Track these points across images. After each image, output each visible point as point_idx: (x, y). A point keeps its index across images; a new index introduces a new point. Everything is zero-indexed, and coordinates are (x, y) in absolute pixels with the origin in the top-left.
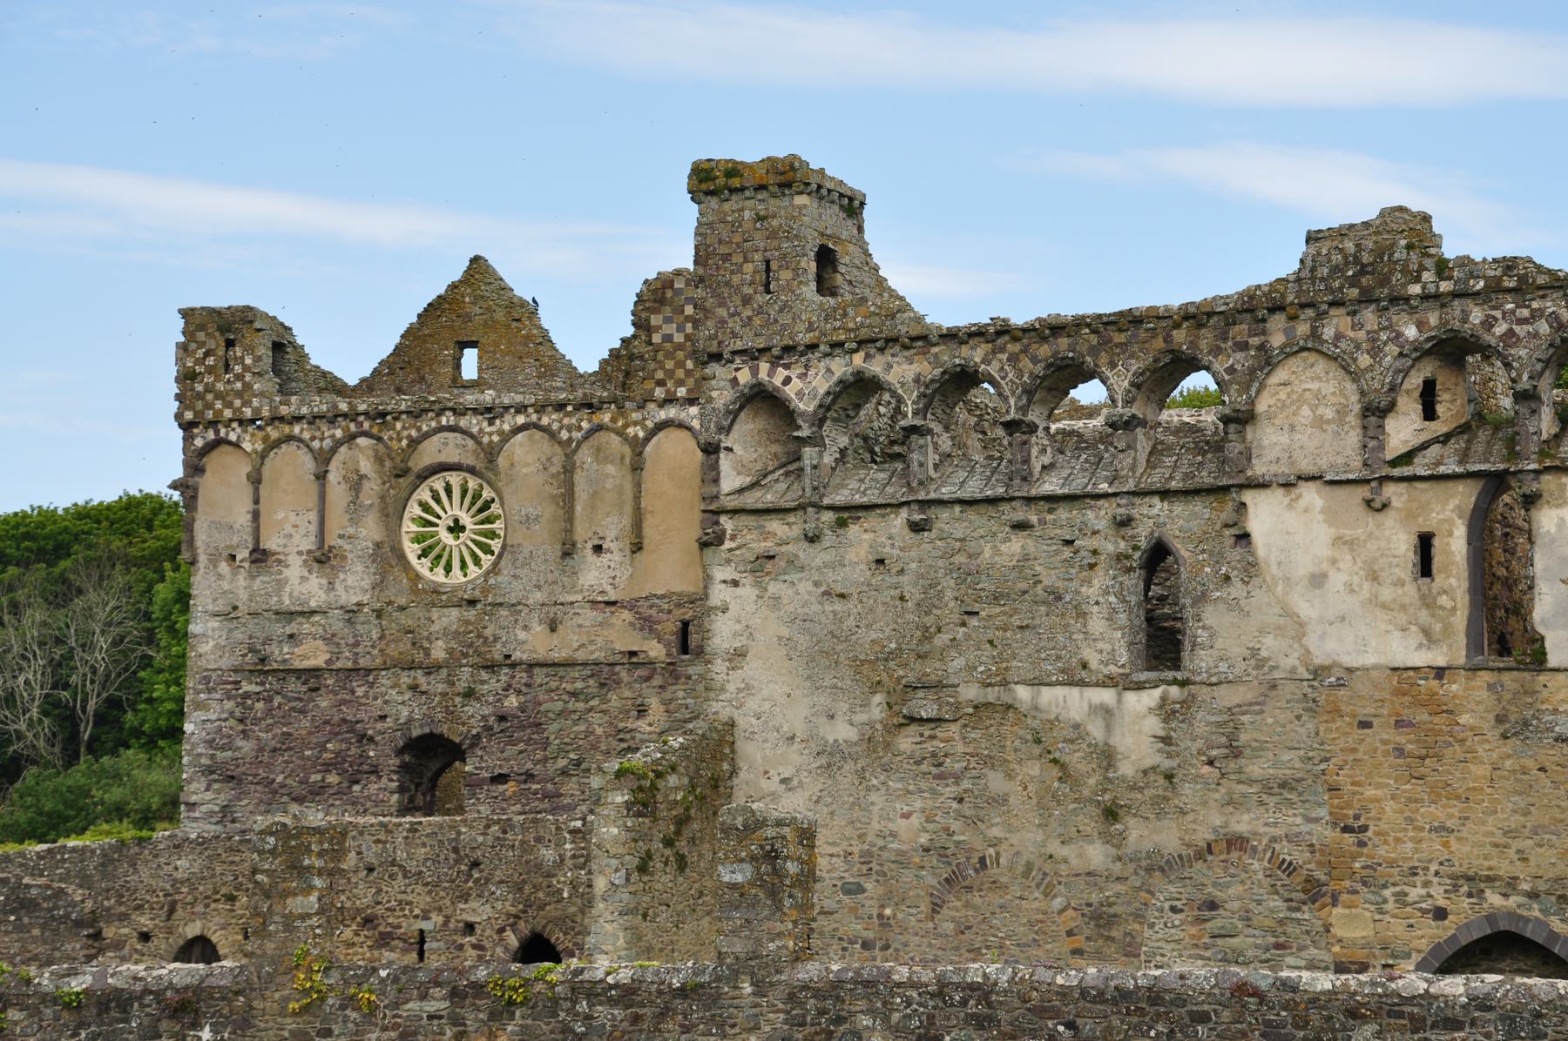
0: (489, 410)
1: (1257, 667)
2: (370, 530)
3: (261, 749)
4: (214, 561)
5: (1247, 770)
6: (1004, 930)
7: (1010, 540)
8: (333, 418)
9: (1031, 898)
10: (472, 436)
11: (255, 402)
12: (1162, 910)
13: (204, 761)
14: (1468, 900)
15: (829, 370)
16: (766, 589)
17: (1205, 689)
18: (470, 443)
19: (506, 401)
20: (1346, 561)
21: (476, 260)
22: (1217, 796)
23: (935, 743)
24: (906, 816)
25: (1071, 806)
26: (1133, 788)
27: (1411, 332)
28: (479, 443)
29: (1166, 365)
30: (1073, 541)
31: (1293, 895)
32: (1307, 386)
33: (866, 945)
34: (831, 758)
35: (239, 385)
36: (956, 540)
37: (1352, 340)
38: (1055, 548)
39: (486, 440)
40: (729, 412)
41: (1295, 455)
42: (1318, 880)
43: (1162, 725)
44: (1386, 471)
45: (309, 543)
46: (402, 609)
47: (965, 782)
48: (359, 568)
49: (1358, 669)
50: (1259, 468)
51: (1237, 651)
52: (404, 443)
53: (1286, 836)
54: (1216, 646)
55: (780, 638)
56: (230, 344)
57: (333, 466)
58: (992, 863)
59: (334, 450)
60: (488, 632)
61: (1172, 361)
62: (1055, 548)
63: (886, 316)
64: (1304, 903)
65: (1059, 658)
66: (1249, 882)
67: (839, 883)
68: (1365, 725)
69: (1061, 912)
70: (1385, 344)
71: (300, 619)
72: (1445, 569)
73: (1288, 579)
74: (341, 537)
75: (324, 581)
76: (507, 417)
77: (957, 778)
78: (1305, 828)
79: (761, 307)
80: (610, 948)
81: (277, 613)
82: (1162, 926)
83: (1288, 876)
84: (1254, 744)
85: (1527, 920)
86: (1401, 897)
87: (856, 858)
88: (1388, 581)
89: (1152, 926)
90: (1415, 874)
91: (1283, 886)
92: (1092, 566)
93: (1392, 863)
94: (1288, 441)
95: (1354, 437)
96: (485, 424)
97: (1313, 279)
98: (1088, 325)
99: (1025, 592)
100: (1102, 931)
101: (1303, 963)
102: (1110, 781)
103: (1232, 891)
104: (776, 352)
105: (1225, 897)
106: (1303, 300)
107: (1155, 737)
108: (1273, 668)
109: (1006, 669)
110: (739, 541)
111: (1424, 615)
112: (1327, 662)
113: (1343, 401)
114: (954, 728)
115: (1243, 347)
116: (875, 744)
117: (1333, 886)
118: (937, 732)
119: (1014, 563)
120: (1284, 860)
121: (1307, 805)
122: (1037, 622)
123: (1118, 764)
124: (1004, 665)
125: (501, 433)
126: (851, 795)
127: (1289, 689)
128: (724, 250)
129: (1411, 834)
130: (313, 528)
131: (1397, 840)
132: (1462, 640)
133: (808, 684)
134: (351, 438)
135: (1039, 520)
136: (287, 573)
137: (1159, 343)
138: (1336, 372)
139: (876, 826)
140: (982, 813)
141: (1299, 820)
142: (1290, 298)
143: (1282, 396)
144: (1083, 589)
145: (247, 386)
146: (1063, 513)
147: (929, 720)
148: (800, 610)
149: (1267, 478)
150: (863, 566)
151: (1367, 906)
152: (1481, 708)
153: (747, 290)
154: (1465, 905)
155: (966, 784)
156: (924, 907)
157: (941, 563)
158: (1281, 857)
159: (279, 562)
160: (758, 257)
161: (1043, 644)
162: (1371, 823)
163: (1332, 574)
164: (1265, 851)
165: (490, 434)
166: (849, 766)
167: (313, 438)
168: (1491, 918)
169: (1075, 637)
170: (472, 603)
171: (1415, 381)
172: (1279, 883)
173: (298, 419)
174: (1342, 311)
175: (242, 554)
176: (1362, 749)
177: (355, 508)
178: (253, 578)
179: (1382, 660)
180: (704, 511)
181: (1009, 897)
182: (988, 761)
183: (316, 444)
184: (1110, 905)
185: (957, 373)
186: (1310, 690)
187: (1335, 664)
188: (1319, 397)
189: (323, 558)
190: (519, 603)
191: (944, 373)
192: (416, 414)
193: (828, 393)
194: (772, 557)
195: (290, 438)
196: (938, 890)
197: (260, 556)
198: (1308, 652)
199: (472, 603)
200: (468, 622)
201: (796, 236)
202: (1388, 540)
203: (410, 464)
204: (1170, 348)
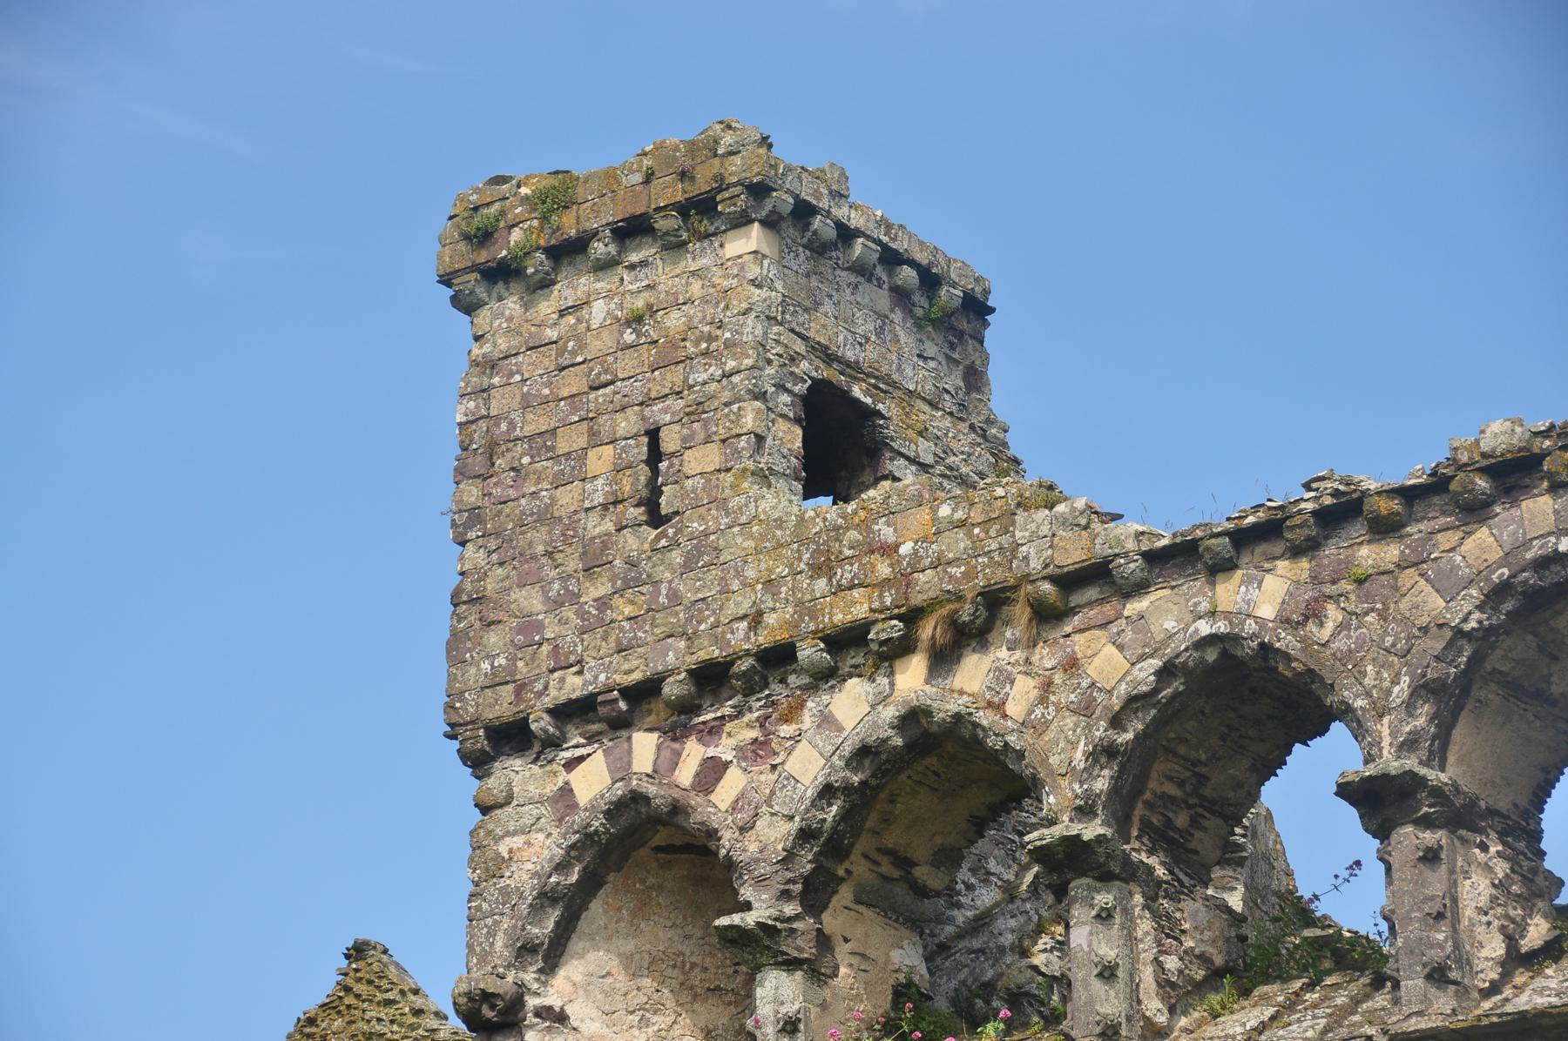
15: (827, 720)
21: (358, 951)
40: (546, 898)
104: (671, 689)
128: (537, 422)
153: (598, 526)
160: (627, 424)
185: (1209, 671)
193: (827, 792)
201: (728, 344)
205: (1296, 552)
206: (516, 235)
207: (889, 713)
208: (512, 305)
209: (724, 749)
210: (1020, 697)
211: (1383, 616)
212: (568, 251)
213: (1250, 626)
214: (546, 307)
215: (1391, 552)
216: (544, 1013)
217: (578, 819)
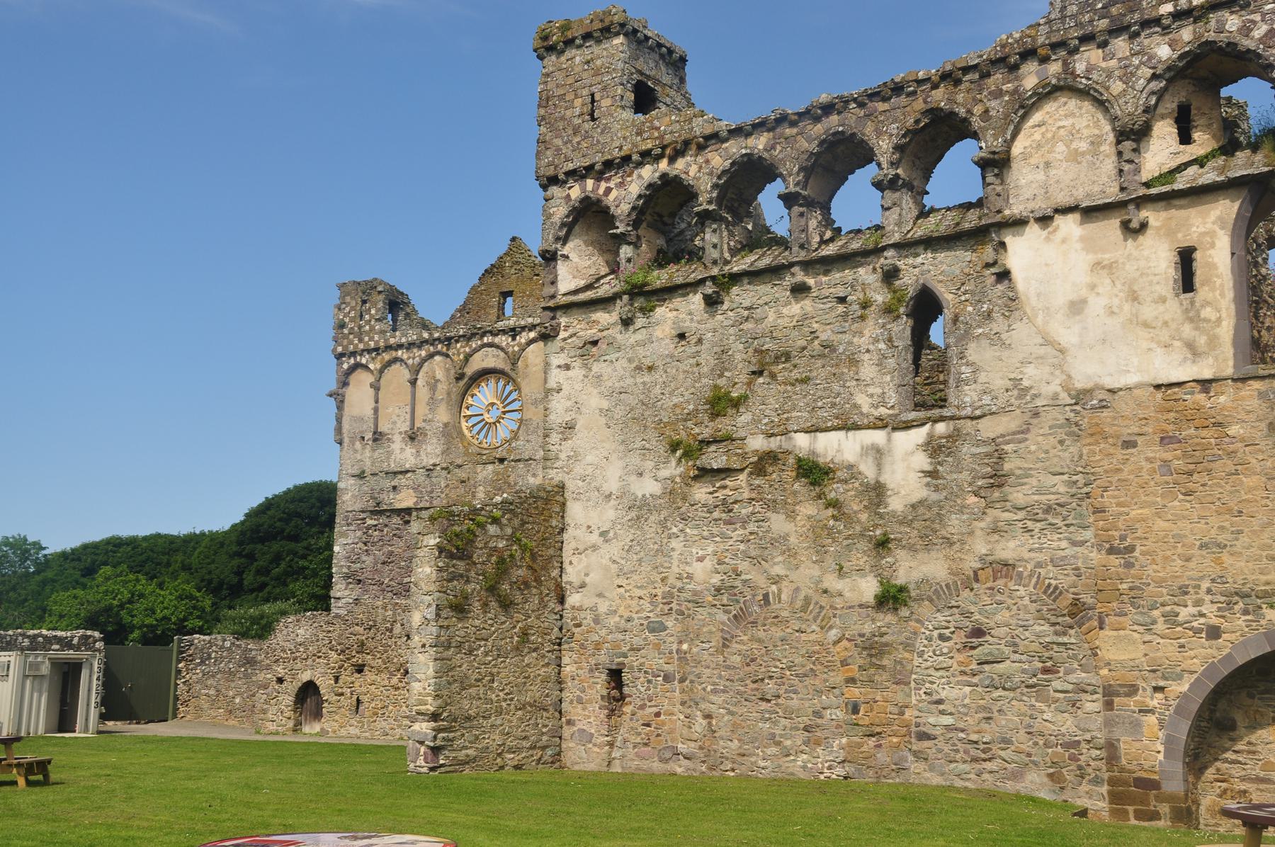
0: (513, 330)
1: (1020, 397)
2: (443, 415)
3: (376, 563)
4: (352, 443)
5: (1010, 497)
6: (784, 661)
7: (790, 304)
8: (422, 343)
9: (809, 631)
10: (502, 349)
11: (376, 338)
12: (930, 639)
13: (345, 570)
14: (1244, 618)
15: (640, 176)
16: (590, 369)
17: (969, 423)
18: (502, 354)
19: (523, 323)
20: (1105, 284)
21: (514, 239)
22: (982, 525)
23: (727, 492)
24: (700, 559)
25: (846, 542)
26: (903, 521)
27: (1164, 52)
28: (506, 353)
29: (926, 125)
30: (846, 297)
31: (1060, 620)
32: (1061, 124)
33: (667, 678)
34: (639, 509)
35: (367, 327)
36: (747, 309)
37: (1103, 70)
38: (830, 305)
39: (510, 349)
40: (563, 225)
41: (1050, 190)
42: (1084, 604)
43: (929, 460)
44: (1142, 191)
45: (405, 427)
46: (459, 466)
47: (751, 525)
48: (435, 441)
49: (1121, 389)
50: (1015, 209)
51: (999, 383)
52: (462, 357)
53: (1052, 561)
54: (980, 380)
55: (601, 410)
56: (364, 302)
57: (420, 376)
58: (774, 599)
59: (421, 365)
60: (511, 479)
61: (932, 122)
62: (830, 305)
63: (685, 121)
64: (1071, 627)
65: (834, 405)
66: (1015, 608)
67: (645, 623)
68: (1129, 444)
69: (836, 643)
70: (1137, 68)
71: (400, 476)
72: (1207, 282)
73: (1048, 308)
74: (424, 421)
75: (414, 451)
76: (524, 334)
77: (744, 523)
78: (1070, 551)
79: (587, 132)
80: (423, 676)
81: (387, 473)
82: (931, 654)
83: (1054, 601)
84: (1018, 472)
86: (1171, 618)
87: (659, 598)
88: (1149, 299)
89: (921, 654)
90: (1186, 593)
91: (1049, 610)
92: (863, 318)
93: (1160, 583)
94: (1044, 178)
95: (1109, 165)
96: (510, 339)
97: (1063, 18)
98: (855, 100)
99: (804, 348)
100: (874, 660)
101: (1070, 687)
102: (881, 516)
103: (998, 618)
104: (597, 167)
105: (992, 624)
106: (1054, 40)
107: (923, 472)
108: (1035, 396)
109: (787, 419)
110: (571, 331)
111: (1187, 330)
112: (1089, 385)
113: (1097, 132)
114: (743, 477)
115: (998, 94)
116: (674, 495)
117: (1100, 608)
118: (727, 482)
119: (794, 323)
120: (1049, 585)
121: (1072, 529)
122: (814, 374)
123: (889, 500)
124: (785, 416)
125: (519, 344)
126: (656, 543)
127: (1052, 416)
128: (561, 92)
129: (1180, 550)
130: (408, 416)
131: (1166, 558)
132: (1228, 350)
133: (622, 448)
134: (431, 356)
135: (816, 282)
136: (393, 446)
137: (919, 105)
138: (1087, 105)
139: (675, 569)
140: (767, 552)
141: (1064, 544)
142: (1041, 40)
143: (1037, 136)
144: (855, 340)
145: (372, 329)
146: (836, 276)
147: (719, 471)
148: (617, 385)
149: (1025, 214)
150: (667, 341)
151: (1136, 627)
152: (1252, 417)
153: (577, 121)
155: (752, 527)
156: (716, 641)
157: (732, 331)
158: (1047, 581)
159: (389, 440)
160: (585, 92)
161: (820, 393)
162: (1138, 543)
163: (1092, 300)
164: (1031, 576)
165: (513, 346)
166: (654, 518)
167: (409, 358)
169: (848, 384)
170: (502, 460)
171: (1170, 105)
173: (400, 346)
174: (1092, 46)
175: (369, 436)
176: (1127, 468)
177: (432, 403)
178: (374, 450)
179: (1147, 378)
180: (545, 309)
181: (789, 630)
182: (772, 505)
183: (410, 362)
184: (882, 635)
186: (1072, 415)
187: (1098, 387)
188: (1073, 133)
189: (413, 437)
190: (531, 459)
191: (733, 164)
192: (468, 338)
193: (640, 196)
194: (595, 343)
195: (396, 360)
196: (728, 626)
197: (378, 437)
198: (1069, 377)
199: (502, 460)
200: (497, 474)
202: (1148, 259)
203: (465, 370)
204: (929, 106)
205: (769, 130)
206: (555, 38)
207: (657, 175)
208: (554, 58)
209: (612, 184)
210: (693, 170)
211: (792, 148)
212: (569, 43)
213: (756, 151)
214: (563, 59)
215: (795, 131)
216: (563, 256)
217: (572, 203)
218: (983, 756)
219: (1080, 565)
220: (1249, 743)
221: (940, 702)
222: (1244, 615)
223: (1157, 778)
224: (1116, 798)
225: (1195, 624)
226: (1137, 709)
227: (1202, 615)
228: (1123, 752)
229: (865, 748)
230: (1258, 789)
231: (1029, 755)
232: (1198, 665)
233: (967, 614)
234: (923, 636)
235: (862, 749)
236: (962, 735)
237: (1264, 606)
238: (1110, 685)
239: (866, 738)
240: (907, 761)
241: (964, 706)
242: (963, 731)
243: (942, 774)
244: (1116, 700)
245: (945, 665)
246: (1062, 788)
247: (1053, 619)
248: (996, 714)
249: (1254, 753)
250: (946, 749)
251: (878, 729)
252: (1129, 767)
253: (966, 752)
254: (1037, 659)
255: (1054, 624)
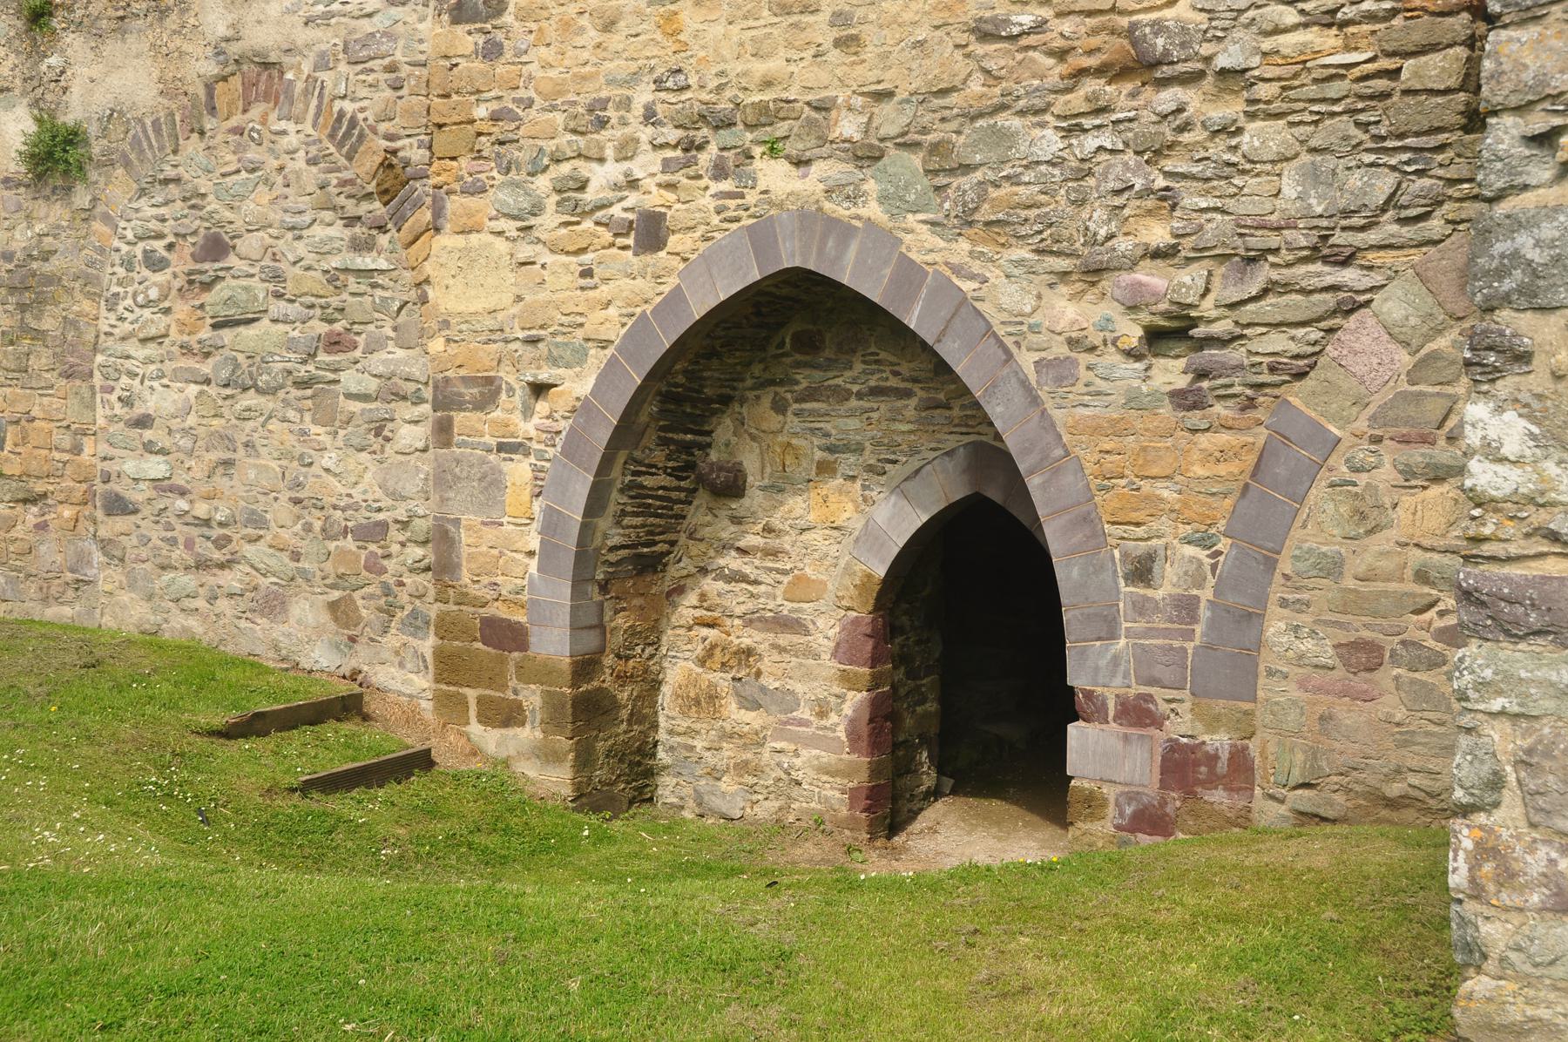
12: (128, 264)
14: (716, 187)
42: (407, 163)
64: (382, 229)
66: (280, 180)
82: (129, 302)
83: (350, 158)
85: (842, 231)
90: (603, 123)
91: (343, 183)
120: (341, 114)
151: (502, 224)
154: (707, 202)
164: (307, 93)
168: (761, 235)
172: (333, 179)
184: (46, 256)
218: (217, 556)
219: (399, 56)
220: (768, 530)
221: (143, 422)
222: (716, 178)
223: (520, 617)
224: (448, 667)
225: (616, 211)
226: (493, 442)
227: (633, 184)
228: (465, 551)
229: (18, 532)
230: (774, 646)
231: (296, 556)
232: (611, 324)
233: (194, 200)
234: (116, 258)
235: (13, 534)
236: (182, 504)
237: (757, 151)
238: (447, 380)
239: (20, 508)
240: (89, 563)
241: (186, 432)
242: (183, 493)
243: (150, 598)
244: (459, 418)
245: (153, 331)
246: (353, 639)
247: (351, 208)
248: (241, 451)
249: (774, 553)
250: (156, 534)
251: (39, 487)
252: (474, 590)
253: (189, 544)
254: (318, 312)
255: (351, 221)
